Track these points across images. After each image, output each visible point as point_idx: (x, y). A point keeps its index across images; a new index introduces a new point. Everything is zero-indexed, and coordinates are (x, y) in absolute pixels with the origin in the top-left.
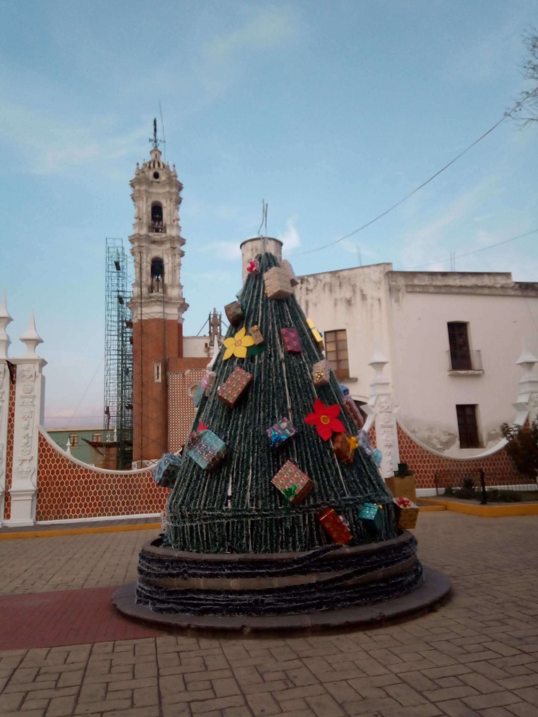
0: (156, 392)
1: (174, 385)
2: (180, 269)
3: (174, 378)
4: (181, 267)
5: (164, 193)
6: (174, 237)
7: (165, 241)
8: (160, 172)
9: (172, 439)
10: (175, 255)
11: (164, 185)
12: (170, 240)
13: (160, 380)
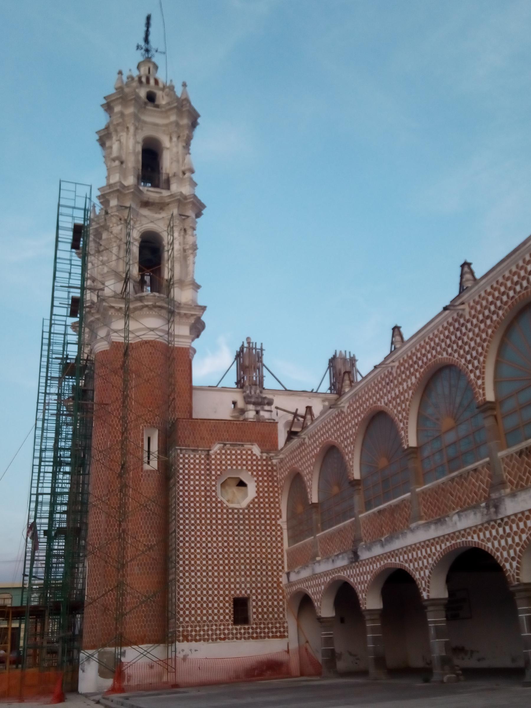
0: (149, 489)
1: (189, 474)
2: (195, 255)
3: (188, 461)
4: (198, 251)
5: (166, 125)
6: (185, 198)
7: (168, 204)
8: (159, 94)
9: (184, 596)
10: (185, 230)
11: (166, 112)
12: (179, 201)
13: (154, 464)
